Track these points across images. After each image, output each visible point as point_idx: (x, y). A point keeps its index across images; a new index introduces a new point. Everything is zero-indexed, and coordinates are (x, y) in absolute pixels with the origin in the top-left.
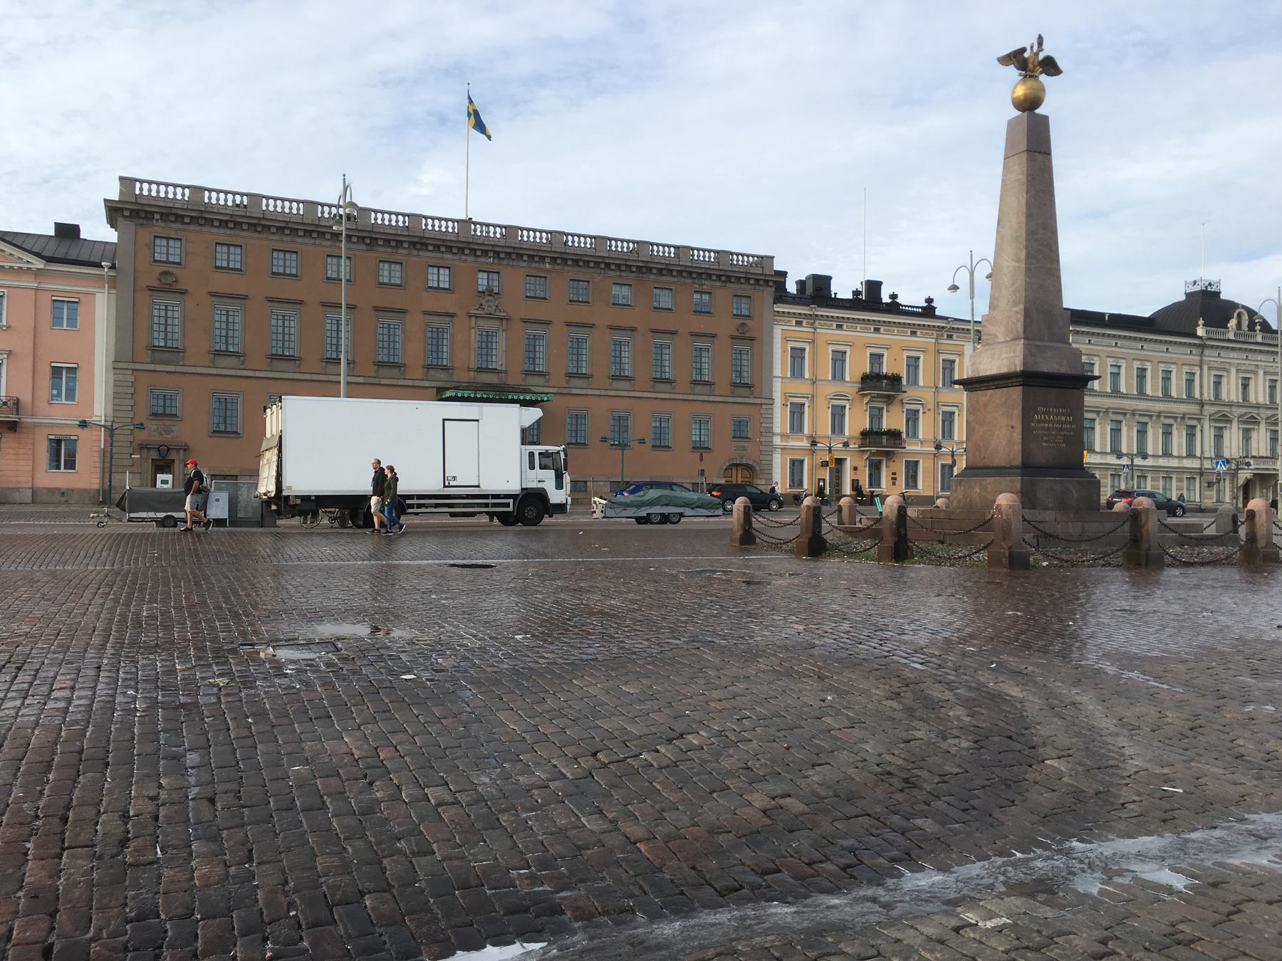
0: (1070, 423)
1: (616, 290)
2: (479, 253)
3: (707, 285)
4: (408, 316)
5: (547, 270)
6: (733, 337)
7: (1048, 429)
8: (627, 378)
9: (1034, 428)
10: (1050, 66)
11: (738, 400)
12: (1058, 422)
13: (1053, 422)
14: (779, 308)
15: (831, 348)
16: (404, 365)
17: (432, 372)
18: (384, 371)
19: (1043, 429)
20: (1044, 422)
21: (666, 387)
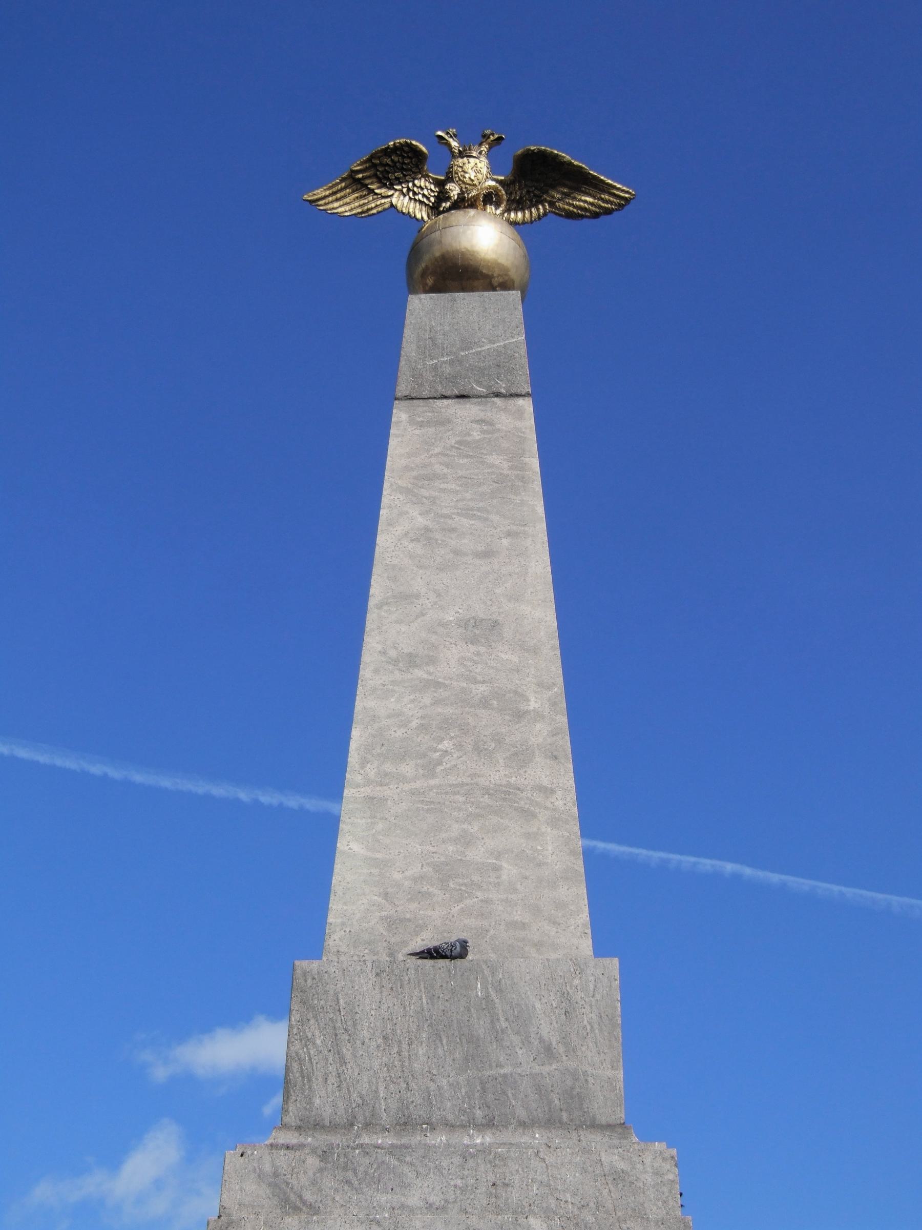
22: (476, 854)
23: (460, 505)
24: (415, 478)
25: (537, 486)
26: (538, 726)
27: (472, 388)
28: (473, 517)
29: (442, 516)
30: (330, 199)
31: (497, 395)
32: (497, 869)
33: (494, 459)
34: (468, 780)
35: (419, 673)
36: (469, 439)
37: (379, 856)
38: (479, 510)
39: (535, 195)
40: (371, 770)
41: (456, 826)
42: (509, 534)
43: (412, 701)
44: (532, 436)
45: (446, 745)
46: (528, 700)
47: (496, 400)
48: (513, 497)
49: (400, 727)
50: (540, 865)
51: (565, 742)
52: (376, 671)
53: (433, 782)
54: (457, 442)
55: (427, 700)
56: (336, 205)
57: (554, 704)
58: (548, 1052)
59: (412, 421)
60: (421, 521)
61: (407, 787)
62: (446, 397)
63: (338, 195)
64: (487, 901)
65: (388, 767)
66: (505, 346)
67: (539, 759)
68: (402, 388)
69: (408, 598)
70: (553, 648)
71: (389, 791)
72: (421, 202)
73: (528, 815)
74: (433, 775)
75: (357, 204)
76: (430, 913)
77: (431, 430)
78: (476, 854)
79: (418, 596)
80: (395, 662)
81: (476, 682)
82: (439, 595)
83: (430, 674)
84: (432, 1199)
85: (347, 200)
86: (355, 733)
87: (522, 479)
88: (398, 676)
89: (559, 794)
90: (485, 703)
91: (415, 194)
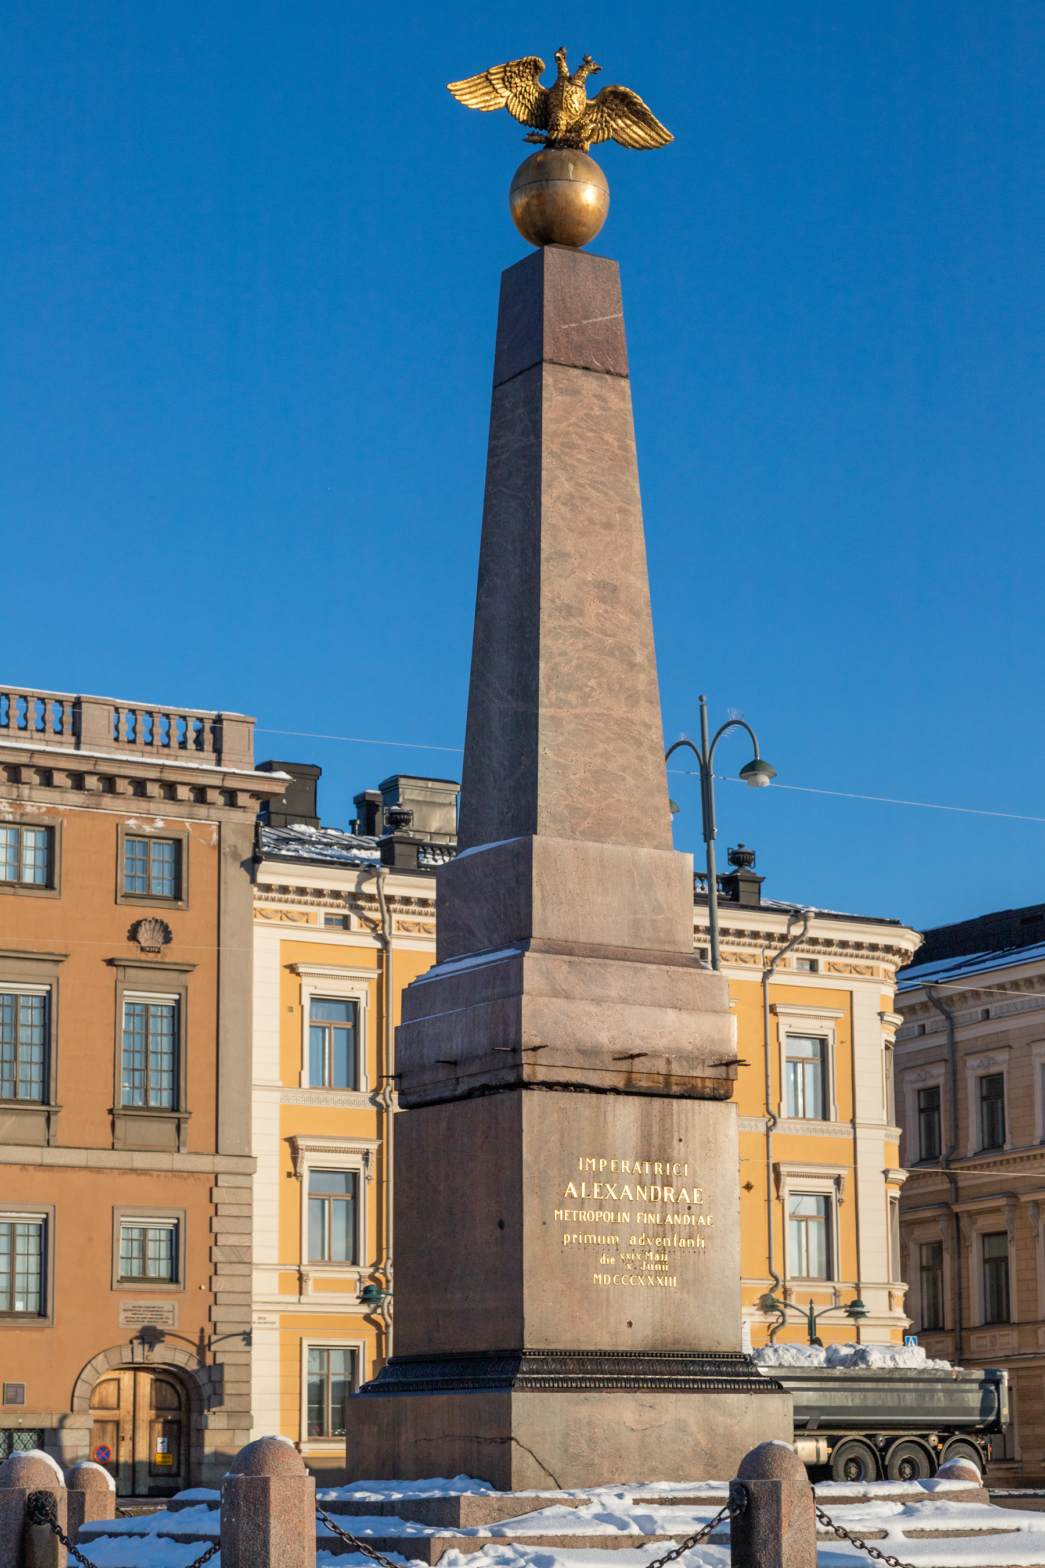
9: (564, 1227)
20: (601, 1207)
23: (590, 476)
24: (562, 444)
25: (635, 469)
26: (642, 676)
27: (592, 362)
28: (597, 489)
29: (579, 485)
30: (466, 91)
31: (608, 372)
32: (624, 779)
33: (609, 437)
34: (605, 712)
35: (574, 622)
36: (593, 413)
37: (561, 760)
38: (602, 483)
39: (606, 121)
40: (553, 695)
41: (601, 745)
42: (621, 510)
43: (572, 644)
44: (631, 419)
45: (592, 683)
46: (635, 655)
47: (607, 376)
48: (621, 475)
49: (566, 664)
50: (646, 779)
51: (656, 690)
52: (550, 616)
53: (587, 710)
54: (586, 415)
55: (580, 646)
56: (468, 97)
57: (649, 661)
59: (555, 386)
60: (568, 487)
61: (573, 711)
62: (576, 367)
63: (472, 89)
64: (618, 801)
65: (562, 695)
66: (611, 321)
67: (642, 702)
68: (548, 352)
69: (564, 556)
70: (648, 615)
71: (563, 713)
72: (526, 107)
73: (640, 744)
74: (585, 705)
75: (482, 99)
76: (590, 805)
77: (568, 398)
78: (612, 767)
79: (569, 555)
80: (559, 609)
81: (606, 635)
82: (582, 557)
83: (581, 624)
84: (621, 993)
85: (476, 94)
86: (542, 664)
87: (626, 459)
88: (563, 623)
89: (654, 729)
90: (612, 654)
91: (524, 98)
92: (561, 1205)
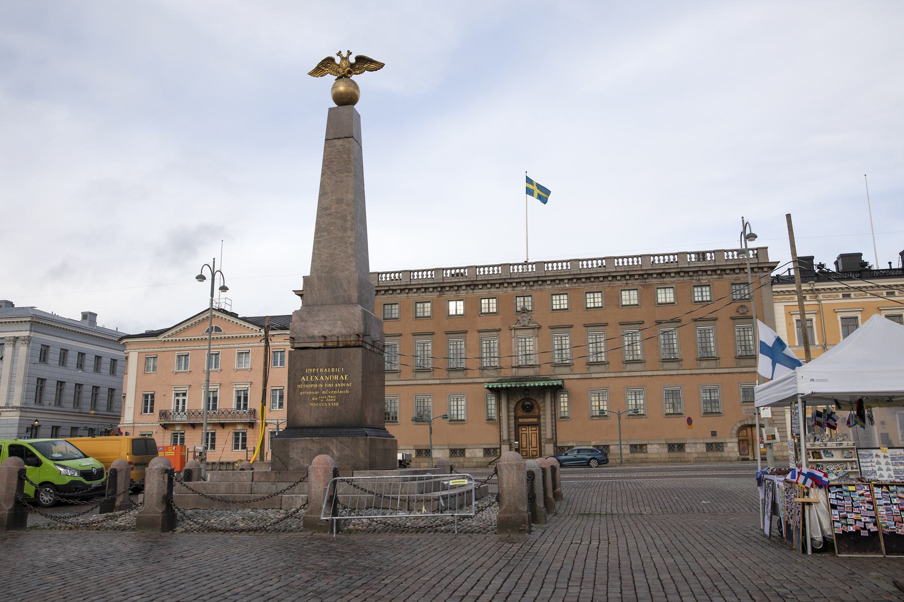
0: (344, 381)
1: (625, 295)
2: (531, 283)
3: (705, 279)
4: (468, 334)
5: (568, 289)
6: (732, 318)
7: (318, 389)
8: (676, 360)
9: (301, 390)
10: (364, 63)
11: (744, 370)
12: (329, 382)
13: (324, 382)
14: (776, 288)
15: (839, 316)
16: (681, 360)
17: (485, 371)
18: (452, 374)
19: (312, 389)
20: (313, 383)
21: (675, 365)
22: (337, 252)
33: (344, 156)
58: (345, 291)
78: (337, 252)
92: (300, 383)
